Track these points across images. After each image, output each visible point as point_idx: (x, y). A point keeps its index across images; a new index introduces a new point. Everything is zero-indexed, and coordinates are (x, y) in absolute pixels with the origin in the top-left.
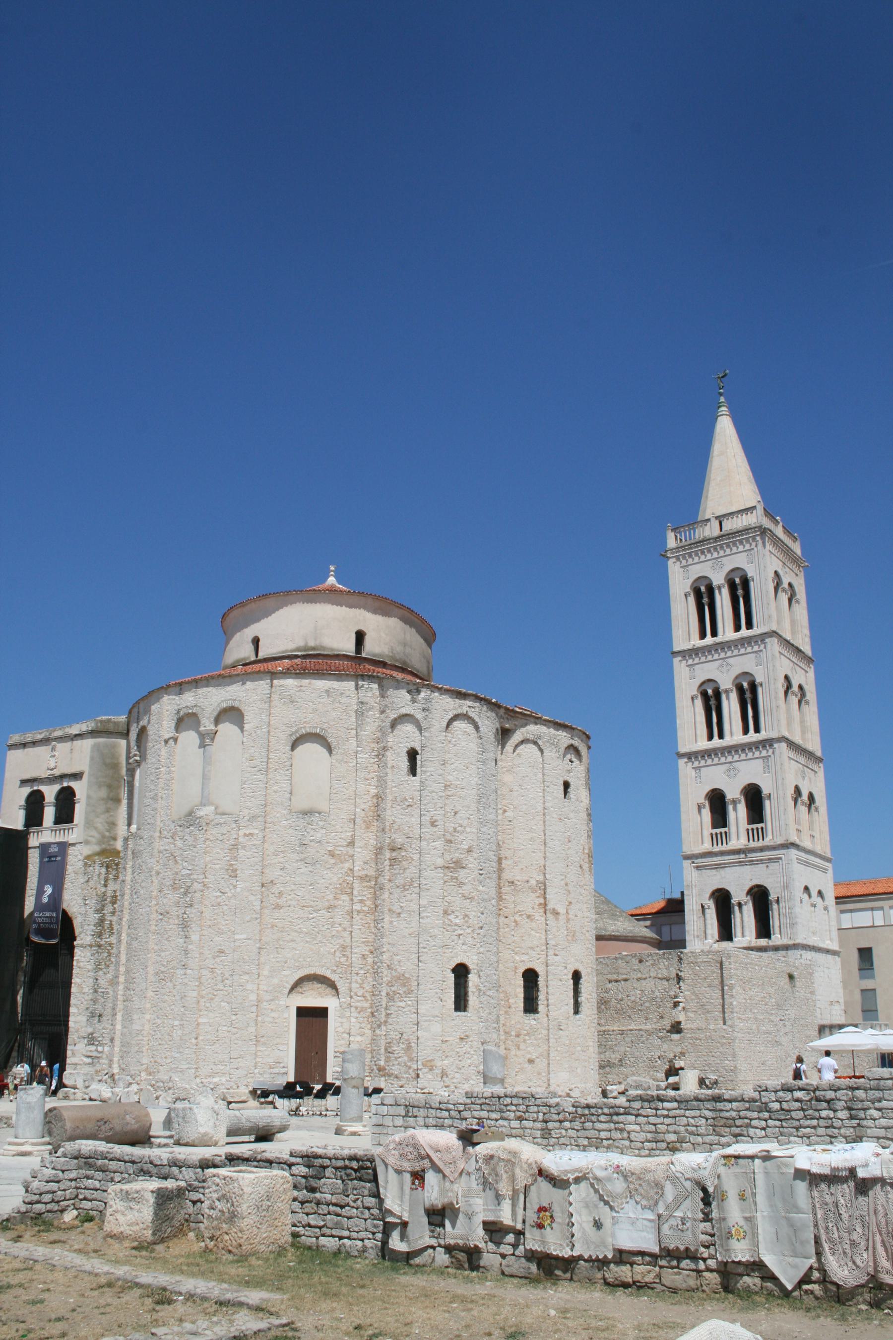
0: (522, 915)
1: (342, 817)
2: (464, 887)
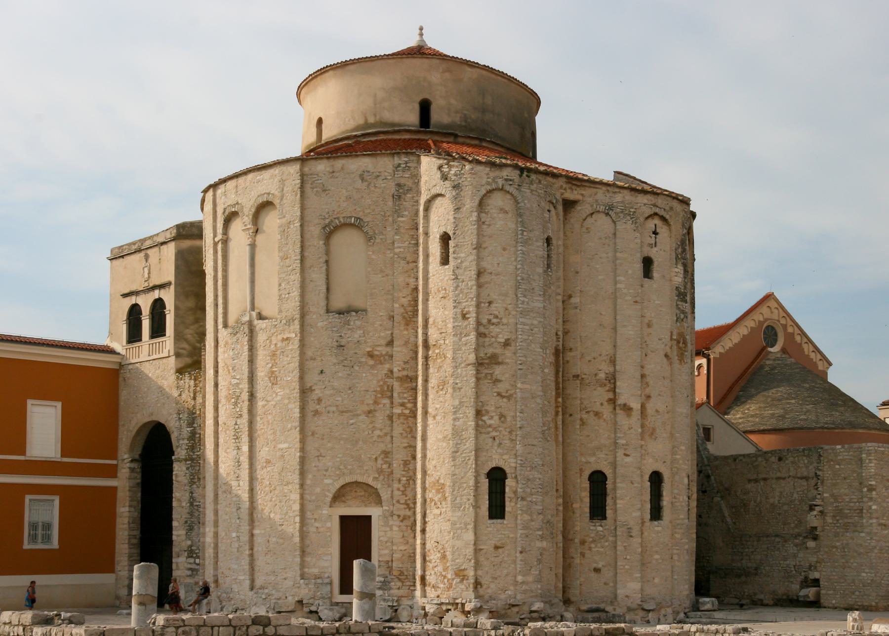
0: (588, 412)
1: (381, 314)
2: (500, 385)
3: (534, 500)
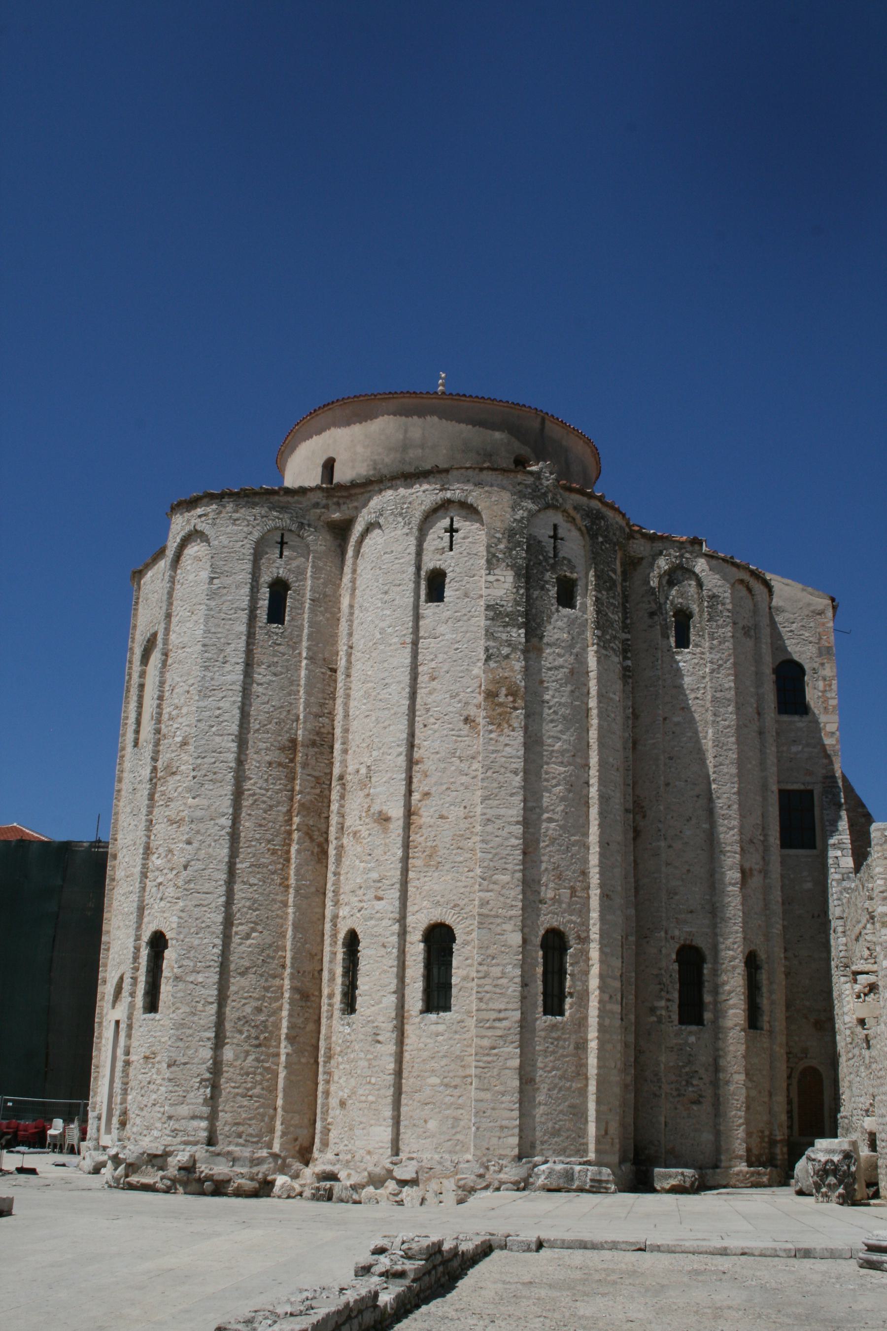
2: (172, 805)
3: (200, 980)
